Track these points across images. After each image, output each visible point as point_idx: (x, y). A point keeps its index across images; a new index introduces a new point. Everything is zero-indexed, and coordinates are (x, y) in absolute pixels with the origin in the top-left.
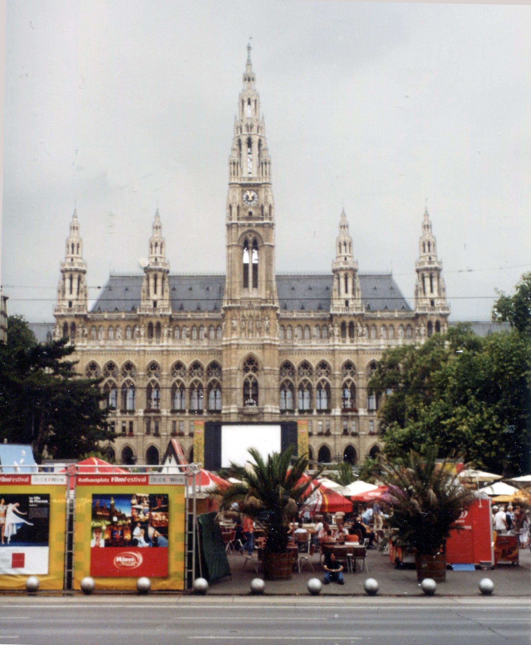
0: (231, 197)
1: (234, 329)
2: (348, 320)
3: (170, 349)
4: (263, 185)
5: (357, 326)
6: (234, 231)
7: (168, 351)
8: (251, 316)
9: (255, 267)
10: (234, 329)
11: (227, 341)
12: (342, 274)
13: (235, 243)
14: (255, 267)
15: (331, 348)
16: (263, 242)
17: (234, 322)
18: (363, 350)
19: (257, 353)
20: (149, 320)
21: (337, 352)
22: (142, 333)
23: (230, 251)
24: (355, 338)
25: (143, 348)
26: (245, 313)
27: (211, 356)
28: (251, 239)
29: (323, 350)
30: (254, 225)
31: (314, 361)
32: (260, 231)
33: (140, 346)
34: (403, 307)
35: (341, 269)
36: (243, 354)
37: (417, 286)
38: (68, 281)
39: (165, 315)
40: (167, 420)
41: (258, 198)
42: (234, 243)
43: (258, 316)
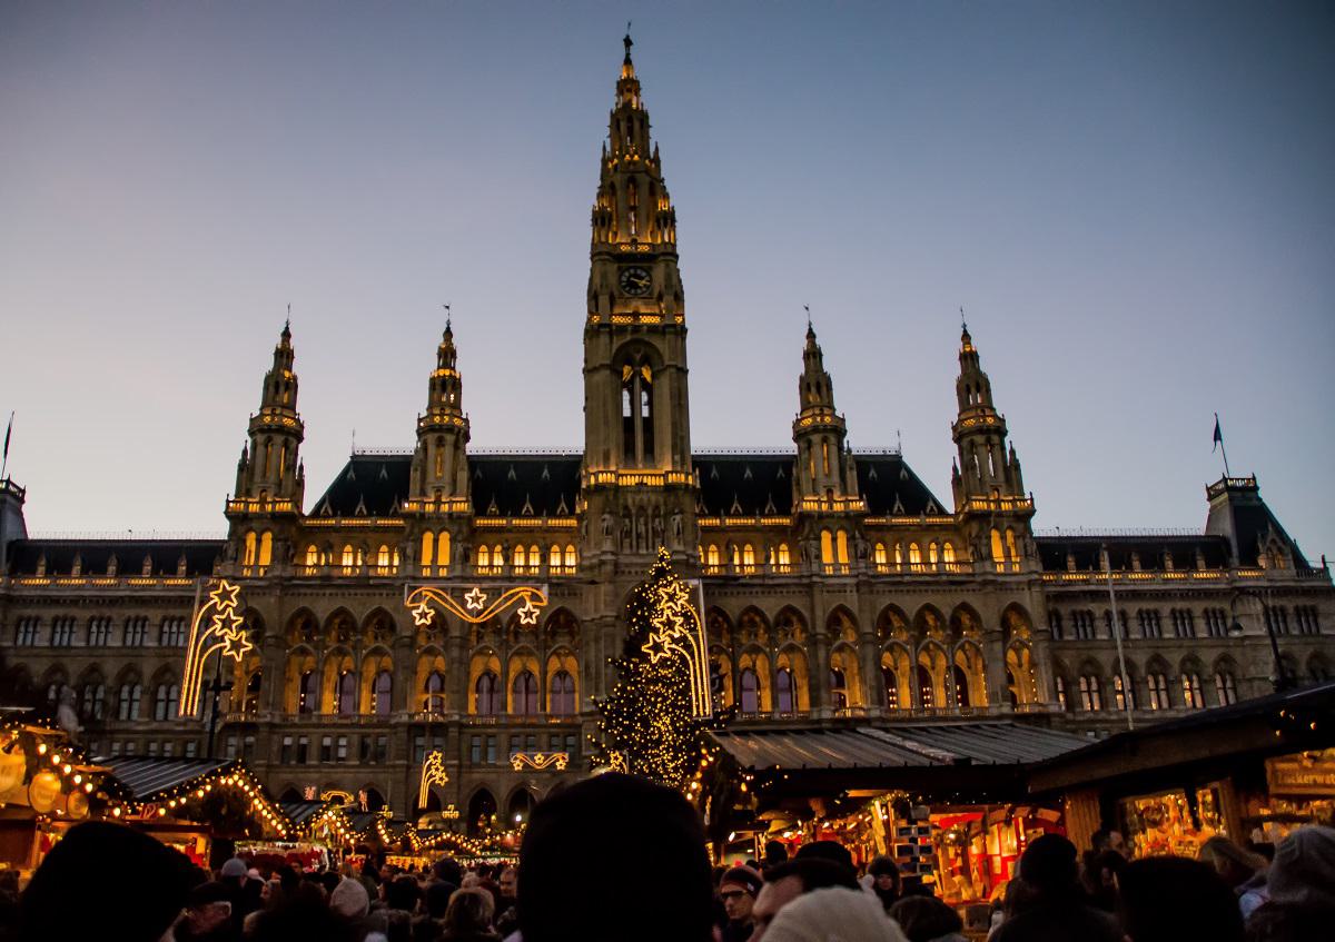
0: (597, 281)
1: (608, 532)
4: (662, 258)
6: (604, 339)
8: (642, 508)
9: (648, 423)
10: (608, 532)
11: (594, 556)
13: (608, 362)
14: (648, 423)
15: (805, 581)
17: (607, 516)
18: (871, 585)
21: (816, 590)
26: (630, 501)
29: (786, 585)
31: (770, 606)
32: (657, 342)
34: (932, 509)
37: (955, 469)
38: (260, 449)
40: (460, 733)
43: (657, 507)
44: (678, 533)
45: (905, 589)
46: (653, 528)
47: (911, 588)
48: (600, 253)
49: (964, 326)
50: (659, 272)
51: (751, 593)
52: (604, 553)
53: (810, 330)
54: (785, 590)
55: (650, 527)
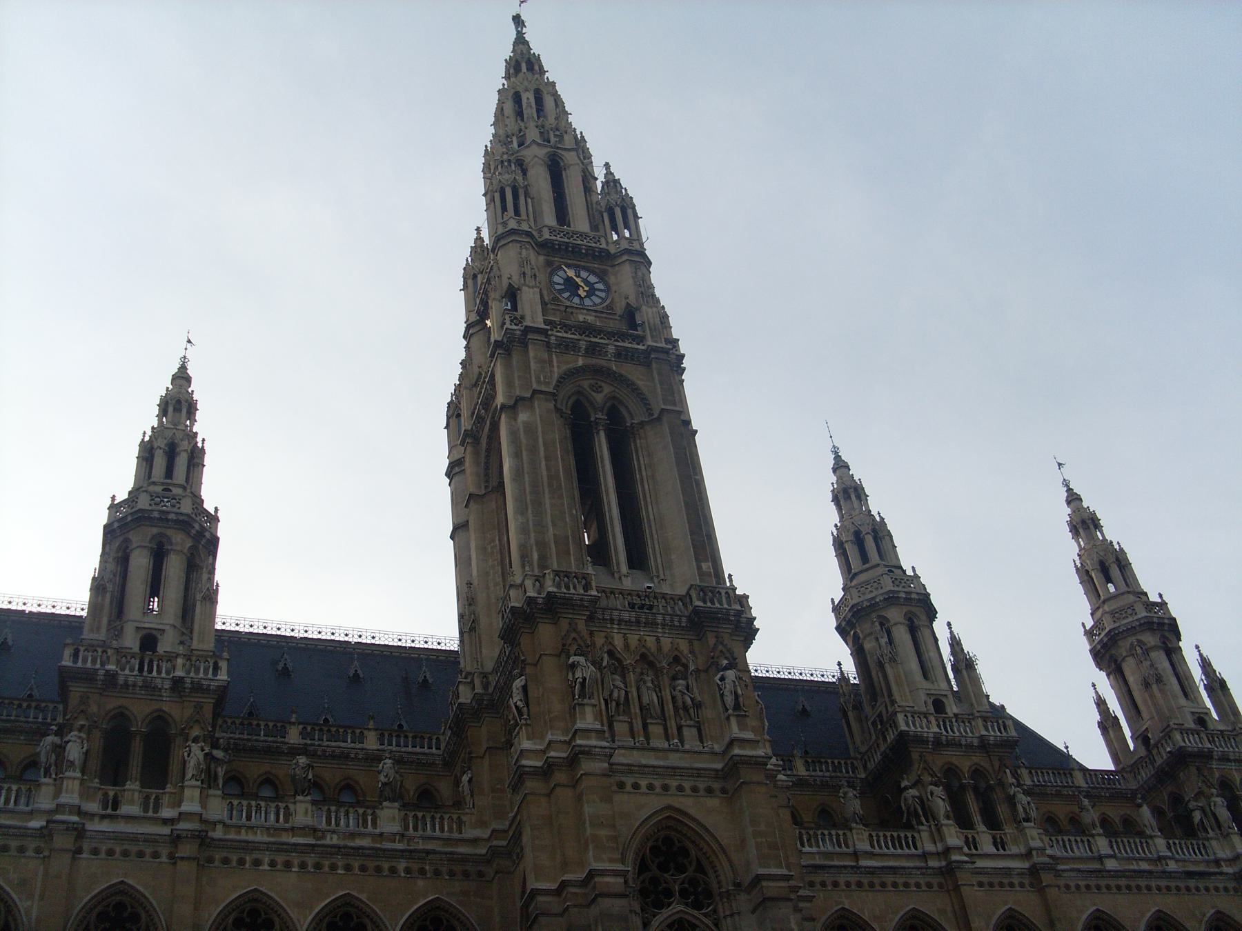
2: (965, 764)
3: (218, 833)
4: (625, 257)
5: (1001, 784)
7: (202, 839)
8: (643, 657)
12: (895, 614)
15: (934, 863)
16: (649, 411)
19: (706, 812)
20: (112, 704)
21: (963, 877)
22: (74, 751)
23: (523, 417)
24: (1009, 830)
25: (75, 818)
26: (618, 642)
27: (421, 883)
28: (599, 398)
30: (611, 349)
33: (59, 808)
35: (891, 599)
36: (643, 807)
37: (1101, 703)
39: (197, 688)
41: (608, 289)
42: (543, 388)
43: (676, 659)
44: (737, 706)
45: (1113, 883)
46: (673, 698)
47: (1123, 882)
48: (513, 232)
49: (1066, 483)
50: (624, 279)
51: (836, 884)
52: (586, 732)
53: (837, 458)
54: (900, 880)
55: (667, 694)
